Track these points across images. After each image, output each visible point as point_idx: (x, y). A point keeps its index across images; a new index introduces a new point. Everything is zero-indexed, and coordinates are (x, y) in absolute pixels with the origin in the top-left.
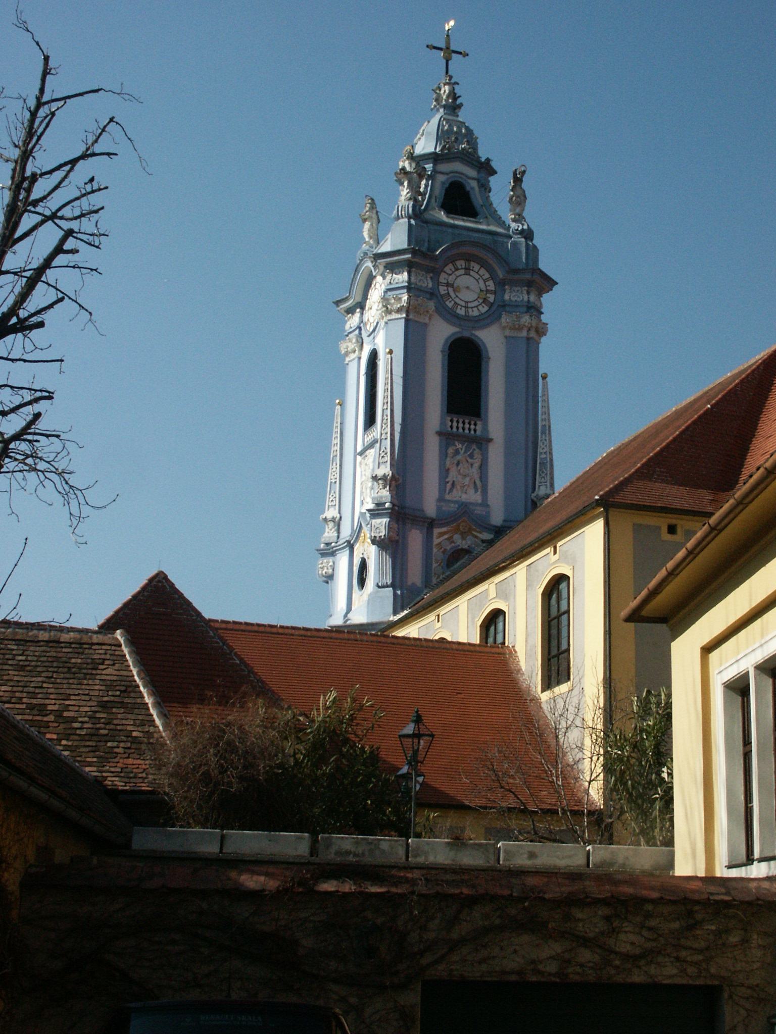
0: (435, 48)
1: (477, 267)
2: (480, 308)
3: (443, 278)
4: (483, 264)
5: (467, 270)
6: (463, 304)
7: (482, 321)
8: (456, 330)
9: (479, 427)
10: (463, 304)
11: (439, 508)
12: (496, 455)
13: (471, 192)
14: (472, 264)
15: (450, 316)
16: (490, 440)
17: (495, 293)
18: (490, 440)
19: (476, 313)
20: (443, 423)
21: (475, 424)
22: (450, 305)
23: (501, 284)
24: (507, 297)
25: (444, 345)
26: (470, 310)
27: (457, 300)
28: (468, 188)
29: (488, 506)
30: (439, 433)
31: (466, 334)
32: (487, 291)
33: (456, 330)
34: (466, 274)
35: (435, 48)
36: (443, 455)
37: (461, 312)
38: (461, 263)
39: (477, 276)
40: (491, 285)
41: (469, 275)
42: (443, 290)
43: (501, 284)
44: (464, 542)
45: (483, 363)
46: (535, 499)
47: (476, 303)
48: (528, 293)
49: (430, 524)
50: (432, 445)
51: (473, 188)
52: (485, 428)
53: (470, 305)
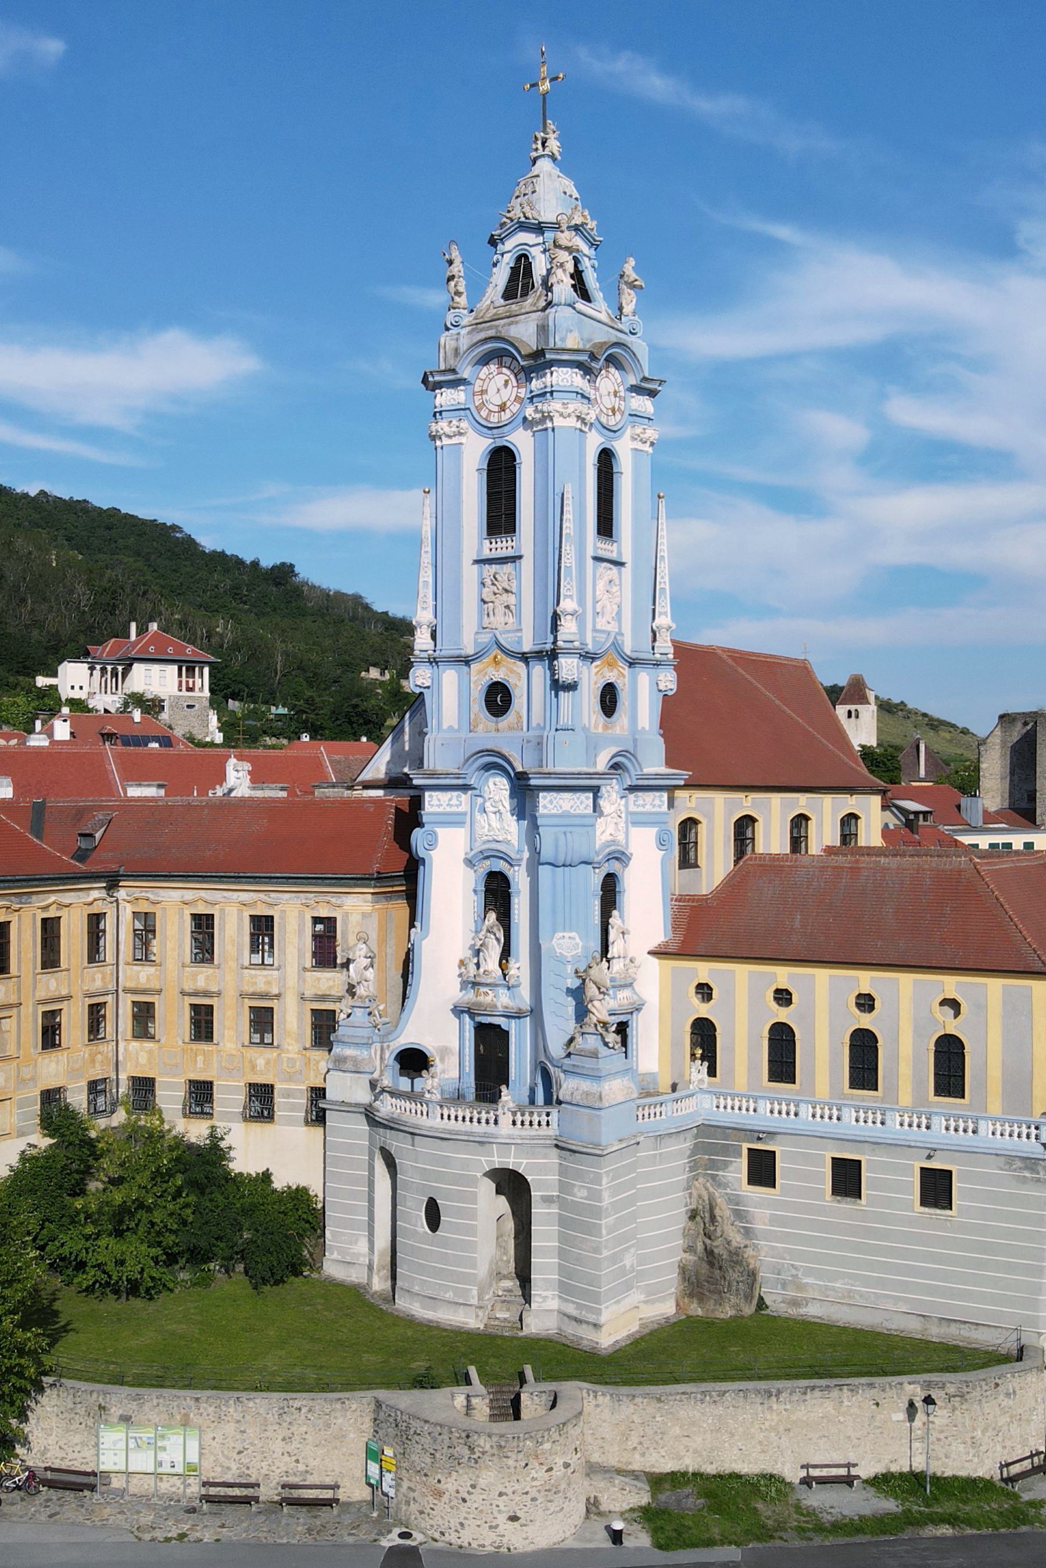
11: (475, 640)
18: (520, 557)
37: (494, 419)
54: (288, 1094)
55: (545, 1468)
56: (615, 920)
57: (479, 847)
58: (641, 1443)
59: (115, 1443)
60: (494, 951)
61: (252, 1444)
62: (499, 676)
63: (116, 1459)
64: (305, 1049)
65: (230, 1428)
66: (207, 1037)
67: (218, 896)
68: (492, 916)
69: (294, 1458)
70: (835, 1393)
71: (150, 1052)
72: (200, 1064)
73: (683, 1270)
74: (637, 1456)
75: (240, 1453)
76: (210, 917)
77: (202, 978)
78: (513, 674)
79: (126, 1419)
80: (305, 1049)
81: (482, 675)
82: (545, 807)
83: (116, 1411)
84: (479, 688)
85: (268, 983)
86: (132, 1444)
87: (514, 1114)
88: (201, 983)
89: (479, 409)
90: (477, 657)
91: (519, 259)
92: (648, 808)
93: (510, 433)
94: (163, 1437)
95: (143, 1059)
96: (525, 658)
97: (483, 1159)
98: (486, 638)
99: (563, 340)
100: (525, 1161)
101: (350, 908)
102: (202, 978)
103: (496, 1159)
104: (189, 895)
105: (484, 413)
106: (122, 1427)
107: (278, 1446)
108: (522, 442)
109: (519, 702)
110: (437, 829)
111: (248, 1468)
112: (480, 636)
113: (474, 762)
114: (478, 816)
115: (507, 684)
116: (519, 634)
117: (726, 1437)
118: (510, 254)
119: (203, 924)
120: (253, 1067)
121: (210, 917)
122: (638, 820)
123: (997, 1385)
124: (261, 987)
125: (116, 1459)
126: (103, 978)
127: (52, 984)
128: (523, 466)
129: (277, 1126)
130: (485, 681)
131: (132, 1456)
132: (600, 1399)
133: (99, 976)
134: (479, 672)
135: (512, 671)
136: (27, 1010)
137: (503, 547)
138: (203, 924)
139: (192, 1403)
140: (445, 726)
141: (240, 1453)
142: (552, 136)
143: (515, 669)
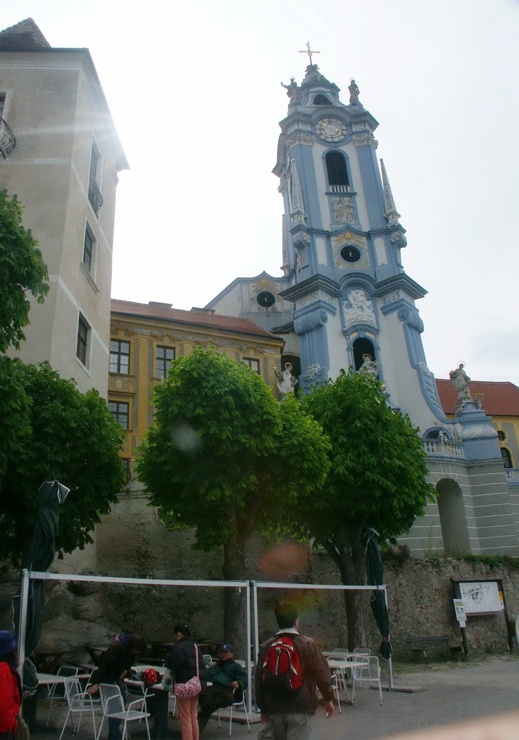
1: (335, 121)
2: (339, 137)
3: (317, 127)
4: (338, 118)
5: (330, 123)
6: (330, 136)
8: (328, 148)
9: (349, 189)
10: (330, 136)
12: (360, 201)
13: (328, 98)
14: (332, 120)
15: (325, 142)
16: (355, 194)
17: (347, 130)
18: (355, 194)
20: (328, 188)
21: (346, 188)
22: (323, 137)
23: (350, 125)
24: (354, 129)
25: (323, 154)
26: (334, 139)
27: (327, 135)
28: (326, 96)
29: (361, 225)
30: (327, 194)
31: (334, 149)
32: (342, 130)
33: (328, 148)
34: (329, 124)
36: (331, 204)
38: (326, 120)
39: (336, 124)
40: (344, 127)
41: (331, 124)
42: (318, 132)
43: (350, 125)
44: (349, 242)
45: (347, 161)
46: (386, 217)
47: (337, 136)
48: (364, 126)
49: (328, 235)
51: (328, 96)
52: (352, 188)
53: (334, 136)
57: (348, 325)
84: (338, 248)
90: (336, 233)
91: (317, 96)
93: (342, 145)
96: (369, 235)
97: (435, 473)
100: (457, 474)
101: (268, 355)
103: (443, 473)
104: (156, 333)
109: (365, 255)
112: (334, 226)
113: (345, 280)
114: (345, 309)
115: (356, 246)
118: (313, 94)
128: (350, 160)
134: (337, 241)
135: (359, 242)
137: (340, 189)
143: (360, 240)
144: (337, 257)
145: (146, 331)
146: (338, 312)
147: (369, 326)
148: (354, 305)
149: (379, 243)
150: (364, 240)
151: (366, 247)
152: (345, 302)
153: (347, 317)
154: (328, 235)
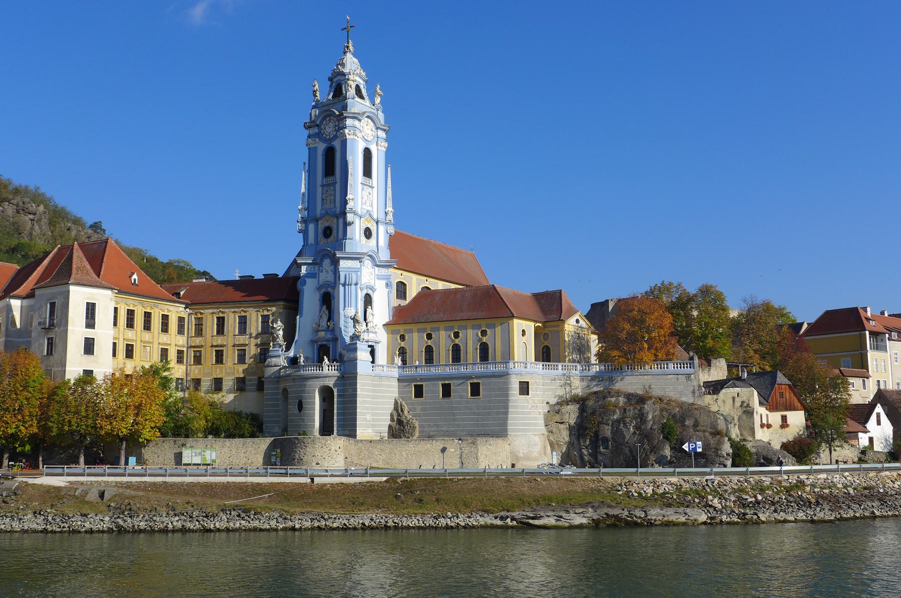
0: (344, 29)
6: (328, 134)
7: (335, 137)
12: (338, 186)
15: (324, 140)
18: (336, 183)
19: (332, 135)
20: (323, 181)
25: (323, 153)
29: (336, 208)
30: (320, 186)
31: (329, 145)
35: (344, 29)
37: (328, 137)
38: (328, 119)
40: (337, 123)
50: (319, 190)
54: (250, 380)
55: (328, 449)
56: (369, 310)
57: (321, 283)
58: (364, 457)
59: (188, 454)
60: (325, 318)
61: (233, 454)
62: (327, 224)
63: (188, 459)
64: (257, 363)
65: (226, 449)
66: (222, 334)
67: (226, 310)
68: (325, 307)
69: (247, 459)
70: (431, 441)
71: (200, 369)
72: (218, 372)
73: (390, 426)
74: (363, 461)
75: (229, 457)
76: (223, 318)
77: (219, 340)
78: (332, 223)
79: (191, 447)
80: (257, 363)
81: (322, 225)
82: (342, 265)
83: (188, 445)
85: (245, 340)
86: (194, 454)
87: (329, 367)
88: (219, 342)
89: (323, 134)
90: (321, 218)
92: (383, 273)
94: (204, 451)
95: (197, 372)
98: (323, 212)
99: (350, 110)
102: (219, 340)
105: (324, 136)
106: (190, 449)
107: (242, 455)
108: (337, 144)
109: (334, 232)
110: (306, 279)
111: (232, 462)
116: (335, 209)
117: (393, 455)
119: (221, 322)
120: (238, 371)
121: (223, 318)
122: (380, 278)
123: (487, 441)
124: (242, 342)
125: (188, 459)
126: (183, 341)
127: (164, 338)
129: (246, 393)
130: (323, 226)
131: (194, 458)
132: (351, 441)
133: (181, 340)
135: (333, 222)
136: (156, 345)
137: (330, 179)
138: (221, 322)
139: (214, 442)
140: (309, 243)
141: (229, 457)
142: (350, 45)
144: (320, 236)
145: (211, 311)
146: (317, 275)
147: (328, 284)
148: (324, 271)
149: (341, 220)
150: (335, 220)
151: (335, 226)
152: (321, 268)
153: (320, 279)
154: (316, 220)
